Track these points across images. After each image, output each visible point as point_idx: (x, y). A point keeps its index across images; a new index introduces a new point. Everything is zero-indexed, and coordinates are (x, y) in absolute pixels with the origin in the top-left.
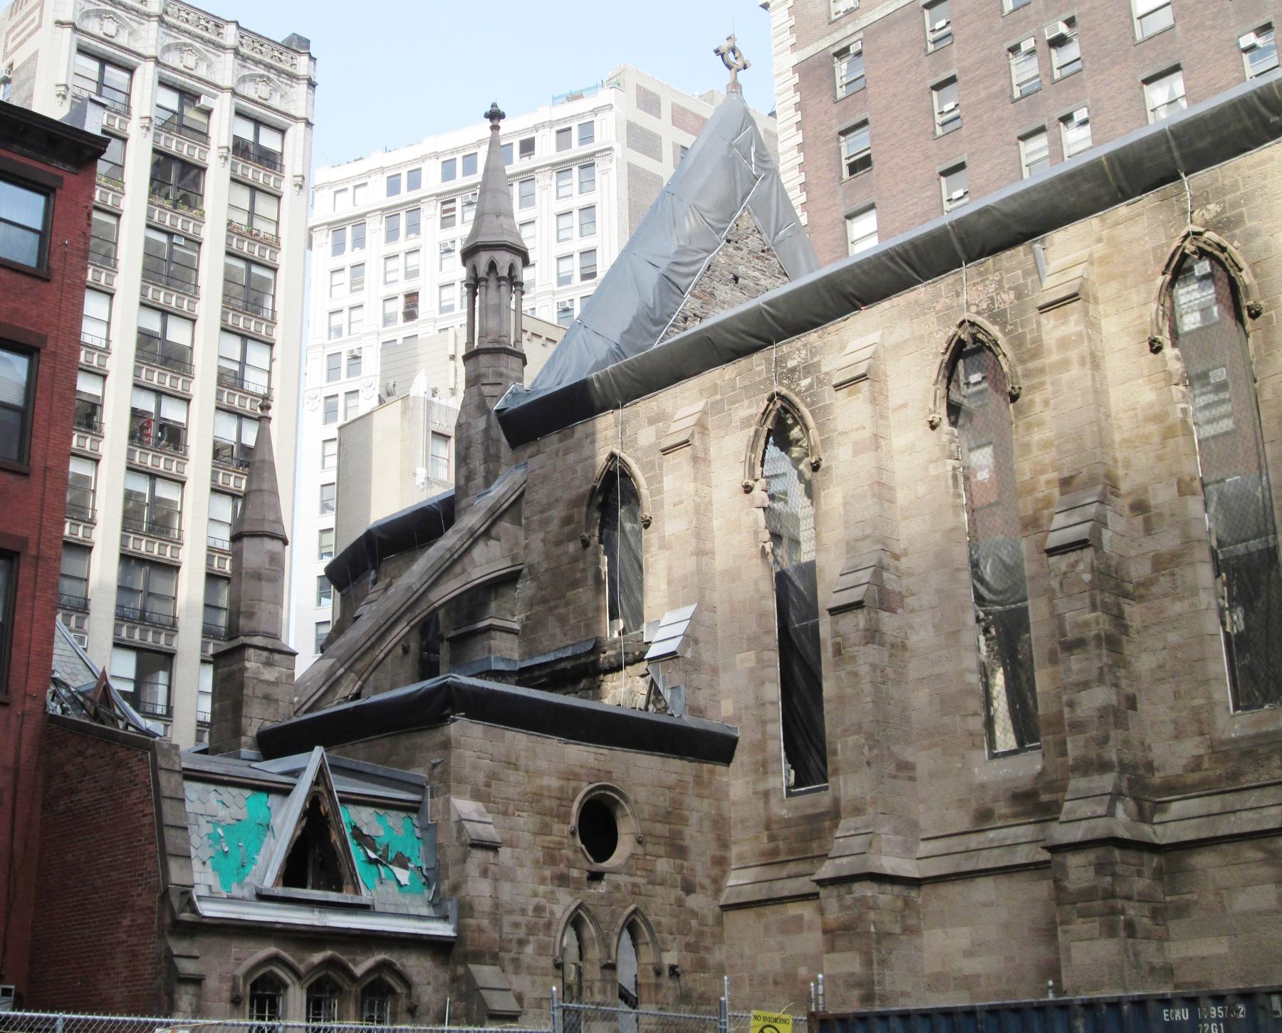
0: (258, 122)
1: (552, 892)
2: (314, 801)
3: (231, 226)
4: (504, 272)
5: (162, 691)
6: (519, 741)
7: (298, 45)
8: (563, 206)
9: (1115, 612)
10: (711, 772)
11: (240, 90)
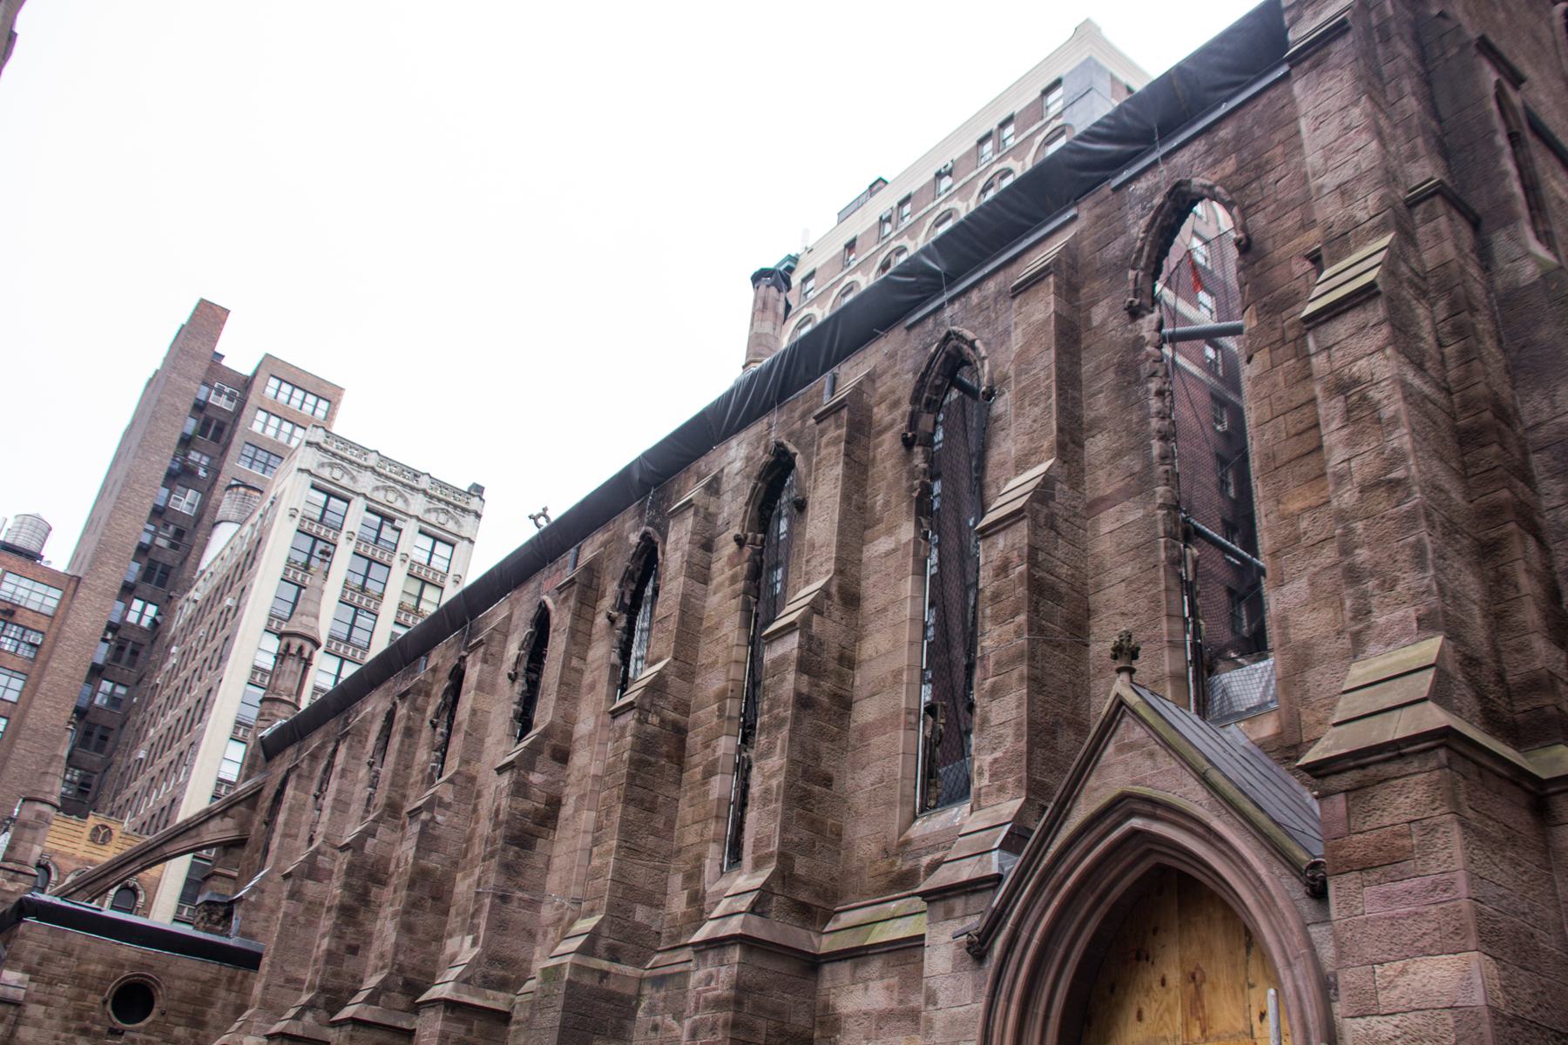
1: (73, 1038)
3: (401, 606)
4: (294, 651)
6: (78, 937)
7: (477, 490)
9: (360, 891)
10: (245, 976)
11: (427, 517)
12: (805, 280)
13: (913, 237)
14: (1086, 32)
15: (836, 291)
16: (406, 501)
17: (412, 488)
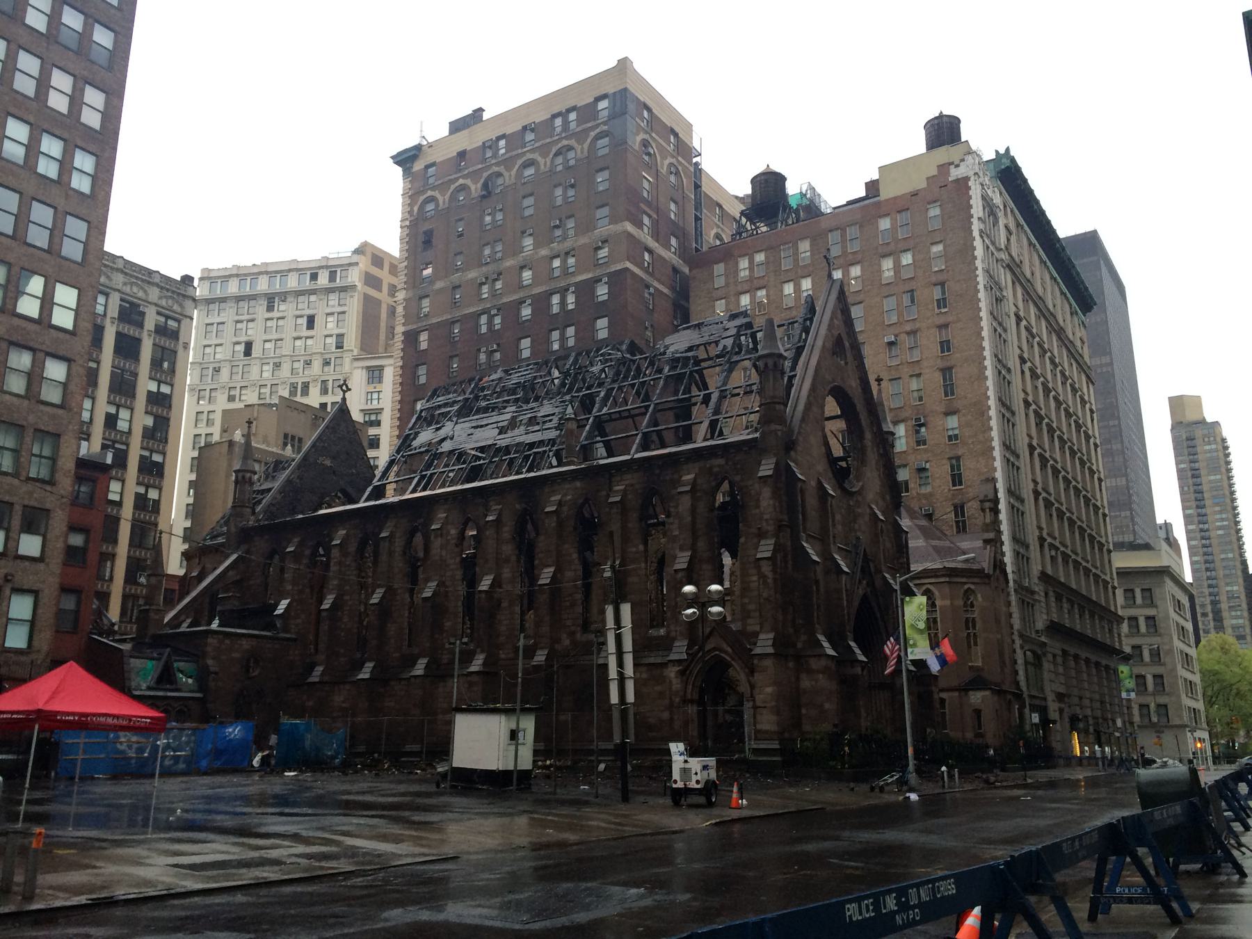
0: (167, 317)
2: (167, 662)
5: (108, 570)
8: (329, 310)
11: (159, 302)
12: (427, 167)
13: (508, 169)
14: (624, 64)
15: (453, 187)
16: (145, 292)
17: (149, 283)
